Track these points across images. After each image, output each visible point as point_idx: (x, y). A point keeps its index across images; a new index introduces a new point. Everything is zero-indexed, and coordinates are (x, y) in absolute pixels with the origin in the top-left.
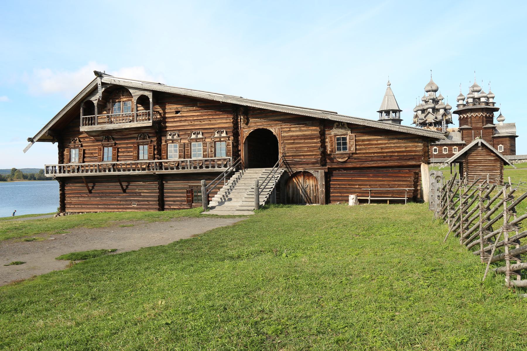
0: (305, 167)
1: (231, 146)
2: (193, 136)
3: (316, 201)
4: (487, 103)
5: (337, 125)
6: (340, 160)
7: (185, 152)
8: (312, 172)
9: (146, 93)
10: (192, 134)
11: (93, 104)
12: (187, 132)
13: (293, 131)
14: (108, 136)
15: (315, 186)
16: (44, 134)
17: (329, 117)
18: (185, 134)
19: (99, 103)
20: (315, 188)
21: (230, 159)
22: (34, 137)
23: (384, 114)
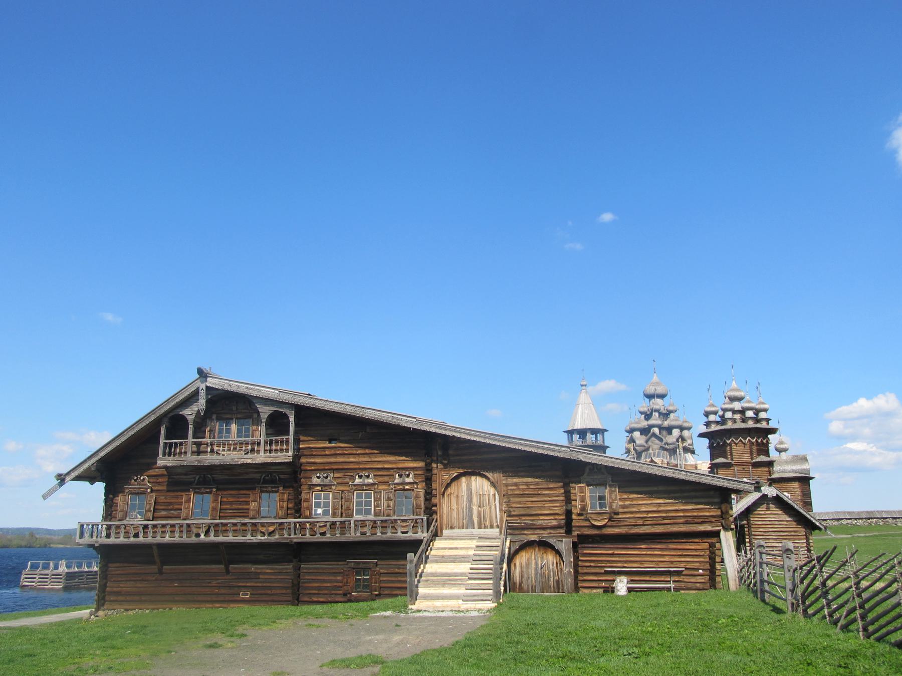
0: (542, 534)
1: (422, 498)
3: (558, 588)
4: (758, 421)
5: (590, 469)
6: (596, 523)
8: (551, 541)
10: (357, 477)
11: (187, 421)
12: (346, 474)
14: (204, 475)
15: (557, 564)
16: (89, 468)
18: (345, 477)
19: (196, 420)
20: (557, 568)
21: (422, 519)
22: (68, 473)
23: (576, 437)
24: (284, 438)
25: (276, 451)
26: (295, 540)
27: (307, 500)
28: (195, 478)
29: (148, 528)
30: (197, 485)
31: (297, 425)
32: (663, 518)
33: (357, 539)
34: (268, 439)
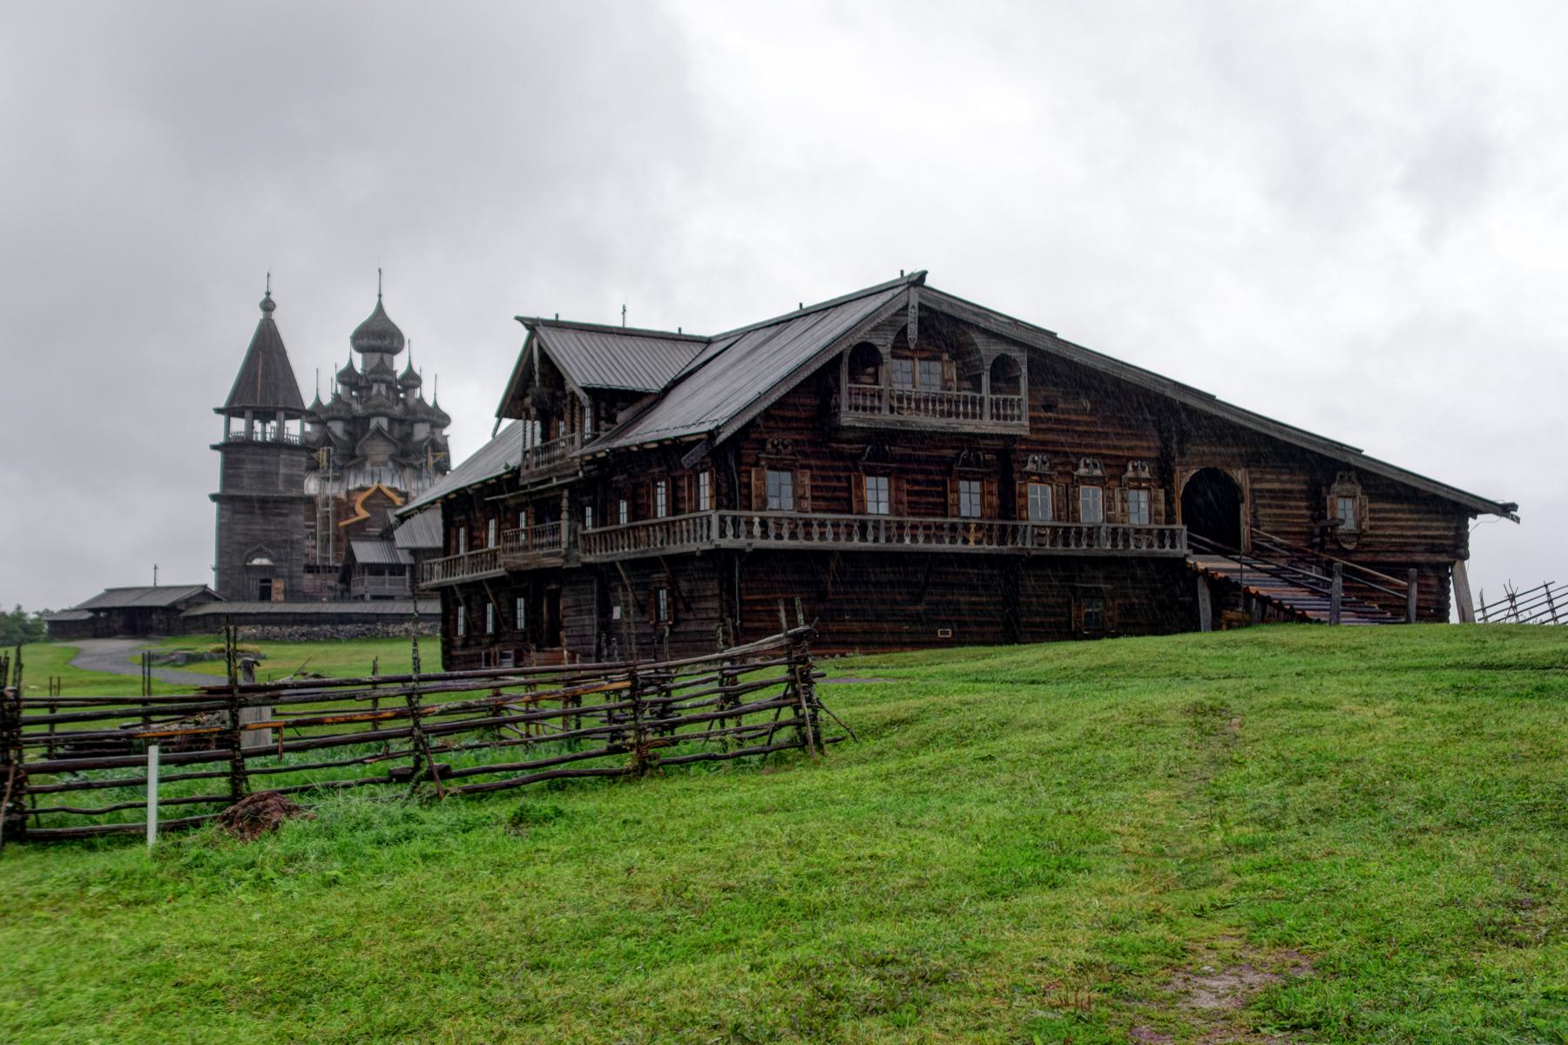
2: (1082, 471)
7: (1067, 505)
9: (1015, 353)
13: (1268, 481)
17: (1351, 460)
24: (1016, 397)
25: (1005, 418)
26: (1033, 553)
27: (1024, 495)
28: (864, 449)
29: (825, 526)
30: (868, 460)
31: (1031, 383)
32: (1406, 544)
33: (1106, 554)
34: (994, 397)
